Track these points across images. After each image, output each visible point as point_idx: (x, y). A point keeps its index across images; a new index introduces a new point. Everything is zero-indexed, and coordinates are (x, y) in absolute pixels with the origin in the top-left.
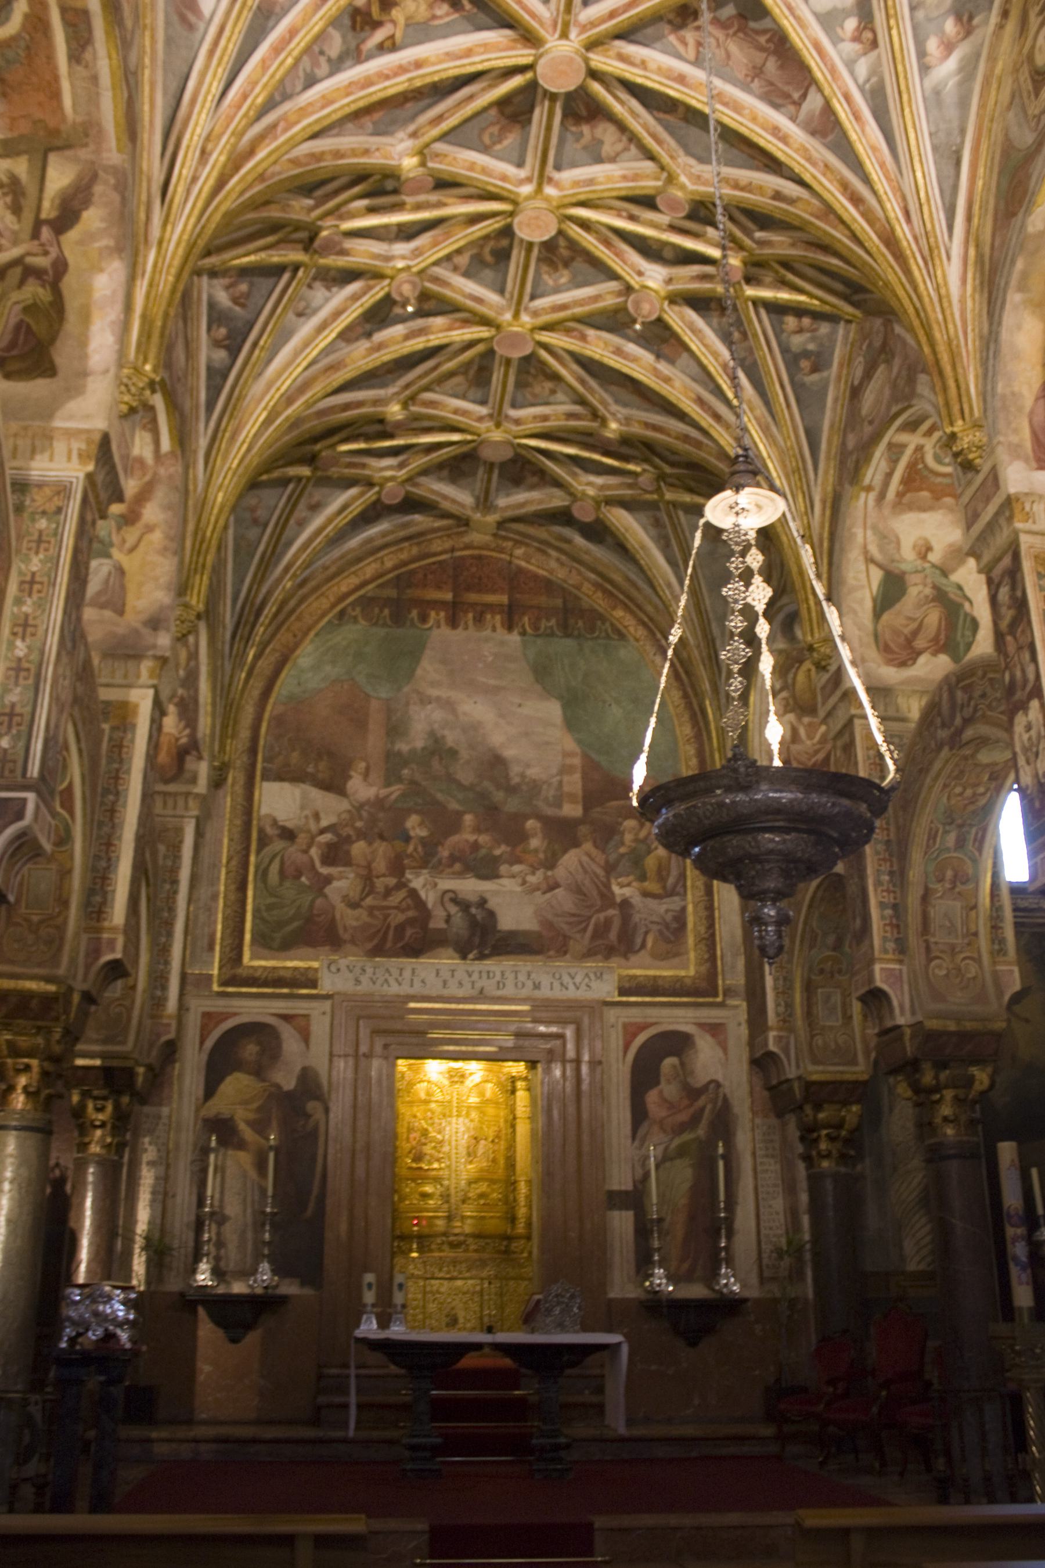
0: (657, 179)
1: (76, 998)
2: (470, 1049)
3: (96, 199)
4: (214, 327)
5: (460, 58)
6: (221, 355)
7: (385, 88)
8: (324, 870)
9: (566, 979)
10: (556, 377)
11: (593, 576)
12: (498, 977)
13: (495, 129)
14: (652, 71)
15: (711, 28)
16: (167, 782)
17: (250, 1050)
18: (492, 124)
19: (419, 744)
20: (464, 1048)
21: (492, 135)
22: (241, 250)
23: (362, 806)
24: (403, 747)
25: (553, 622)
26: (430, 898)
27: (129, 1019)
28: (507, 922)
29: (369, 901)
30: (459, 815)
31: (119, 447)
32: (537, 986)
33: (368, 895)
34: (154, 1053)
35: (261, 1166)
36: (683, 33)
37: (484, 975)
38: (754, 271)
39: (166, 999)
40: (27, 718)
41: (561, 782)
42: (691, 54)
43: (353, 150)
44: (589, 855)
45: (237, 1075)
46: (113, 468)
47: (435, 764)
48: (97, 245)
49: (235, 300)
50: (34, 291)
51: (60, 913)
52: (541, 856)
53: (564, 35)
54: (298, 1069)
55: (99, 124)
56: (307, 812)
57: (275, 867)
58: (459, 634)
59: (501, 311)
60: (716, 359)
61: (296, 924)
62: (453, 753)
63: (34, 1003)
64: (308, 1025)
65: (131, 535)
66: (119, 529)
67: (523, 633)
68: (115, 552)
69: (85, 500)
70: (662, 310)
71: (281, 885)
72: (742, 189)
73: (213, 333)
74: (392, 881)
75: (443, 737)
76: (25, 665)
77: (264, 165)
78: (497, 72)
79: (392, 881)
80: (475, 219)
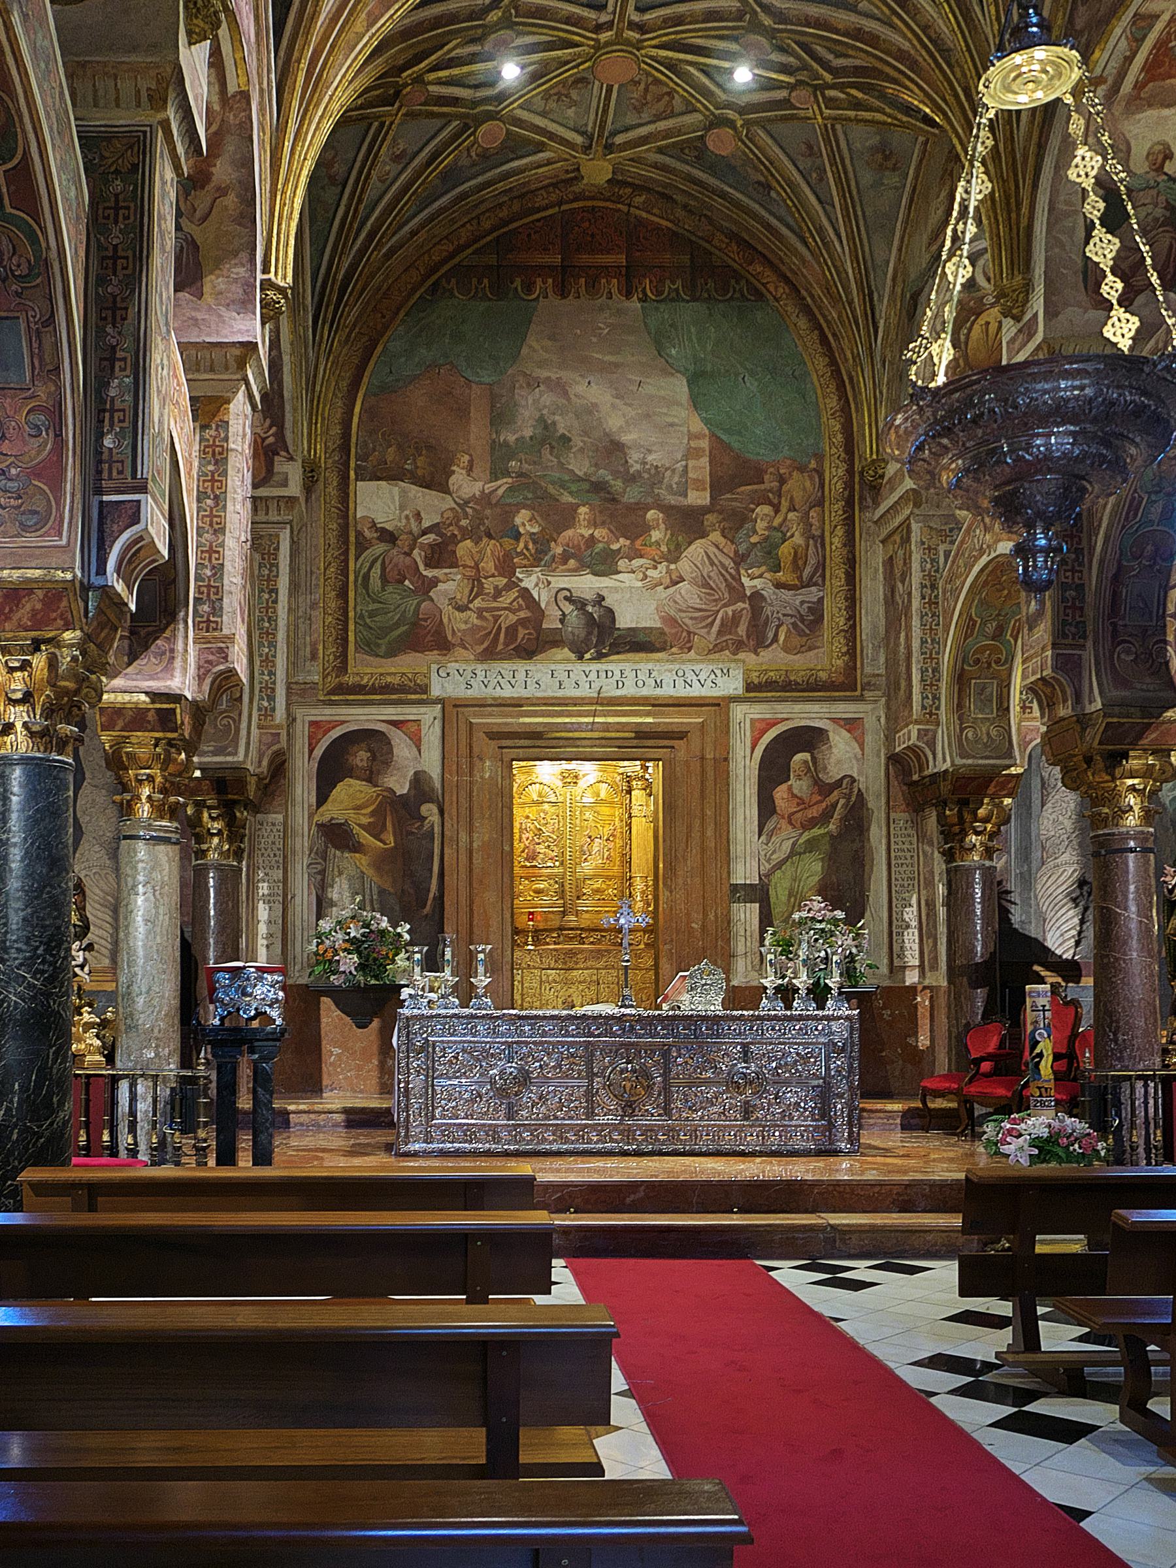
9: (690, 676)
26: (543, 597)
27: (238, 730)
28: (625, 620)
30: (574, 508)
32: (658, 684)
39: (273, 709)
40: (129, 414)
47: (546, 451)
52: (664, 548)
62: (565, 440)
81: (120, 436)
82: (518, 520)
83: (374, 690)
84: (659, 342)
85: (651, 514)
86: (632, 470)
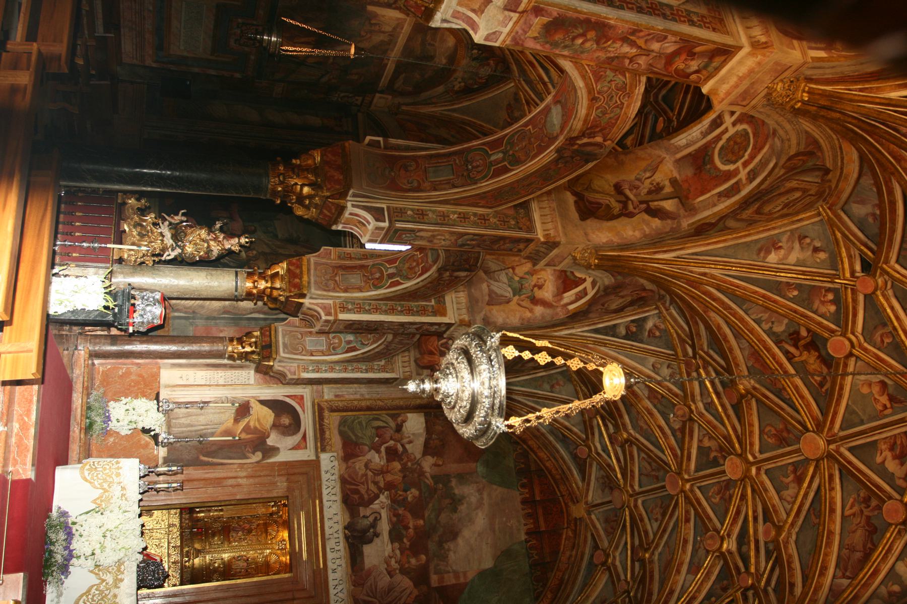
0: (779, 522)
1: (301, 301)
2: (296, 536)
3: (664, 222)
4: (635, 325)
5: (797, 393)
6: (623, 331)
7: (768, 358)
8: (383, 449)
10: (664, 515)
11: (566, 577)
12: (337, 548)
13: (774, 432)
14: (830, 494)
15: (864, 517)
16: (415, 361)
17: (286, 420)
18: (776, 430)
19: (456, 491)
20: (296, 532)
21: (770, 431)
22: (673, 323)
23: (419, 465)
24: (454, 483)
25: (536, 557)
26: (376, 506)
28: (367, 549)
29: (370, 474)
30: (423, 517)
31: (557, 256)
32: (334, 571)
33: (372, 472)
34: (280, 368)
35: (227, 433)
36: (856, 505)
37: (337, 540)
38: (750, 593)
39: (308, 372)
40: (422, 221)
41: (449, 572)
42: (847, 513)
43: (736, 357)
44: (410, 594)
45: (273, 415)
46: (547, 254)
48: (644, 227)
49: (650, 331)
50: (616, 207)
51: (341, 289)
52: (407, 566)
53: (829, 443)
54: (278, 446)
55: (696, 214)
56: (412, 437)
57: (381, 424)
58: (519, 506)
59: (688, 473)
60: (696, 592)
61: (353, 438)
62: (455, 510)
63: (297, 280)
64: (301, 449)
65: (526, 303)
66: (528, 297)
67: (527, 541)
68: (517, 297)
69: (529, 241)
70: (714, 552)
71: (373, 428)
72: (789, 566)
73: (632, 324)
74: (382, 484)
75: (463, 504)
76: (446, 219)
77: (710, 306)
78: (800, 418)
79: (382, 484)
80: (727, 438)
81: (411, 216)
82: (413, 490)
83: (321, 425)
84: (506, 555)
85: (423, 557)
86: (444, 544)
